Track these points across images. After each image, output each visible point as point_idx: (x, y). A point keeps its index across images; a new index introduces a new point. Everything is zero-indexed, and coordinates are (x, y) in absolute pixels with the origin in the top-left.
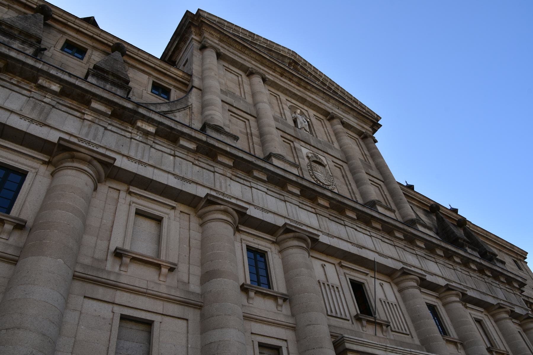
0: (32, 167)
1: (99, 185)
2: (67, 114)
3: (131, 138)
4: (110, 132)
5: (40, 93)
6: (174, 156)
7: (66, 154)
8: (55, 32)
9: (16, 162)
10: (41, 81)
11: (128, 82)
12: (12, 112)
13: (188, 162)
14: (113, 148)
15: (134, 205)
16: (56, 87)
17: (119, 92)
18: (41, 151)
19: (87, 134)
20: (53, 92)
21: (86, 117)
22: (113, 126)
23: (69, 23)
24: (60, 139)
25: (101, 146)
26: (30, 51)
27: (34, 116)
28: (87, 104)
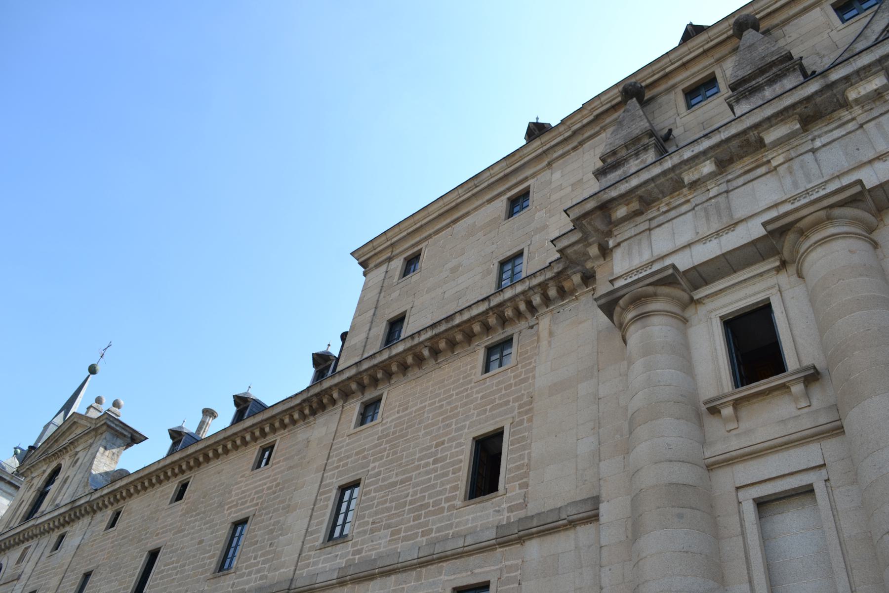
0: (769, 289)
1: (875, 236)
2: (751, 184)
3: (861, 126)
4: (824, 149)
5: (699, 192)
7: (791, 237)
8: (664, 99)
9: (745, 298)
10: (688, 178)
11: (789, 57)
12: (689, 245)
14: (846, 166)
16: (708, 167)
17: (788, 82)
18: (763, 257)
19: (795, 184)
20: (712, 176)
21: (774, 163)
22: (819, 136)
23: (668, 70)
24: (764, 225)
25: (826, 182)
26: (650, 156)
27: (715, 226)
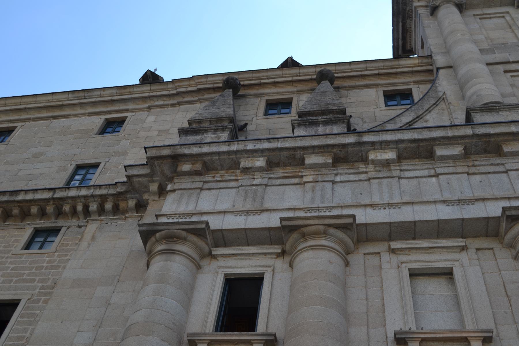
0: (267, 266)
1: (350, 258)
2: (284, 187)
3: (369, 179)
4: (340, 184)
5: (247, 177)
6: (436, 175)
7: (295, 236)
8: (252, 100)
9: (248, 267)
10: (244, 163)
11: (344, 112)
12: (224, 212)
13: (460, 175)
14: (350, 202)
15: (404, 265)
16: (260, 162)
17: (337, 129)
18: (271, 242)
19: (313, 200)
20: (260, 169)
21: (305, 179)
22: (341, 174)
23: (263, 81)
24: (282, 219)
25: (333, 207)
26: (224, 136)
27: (248, 206)
28: (302, 162)
